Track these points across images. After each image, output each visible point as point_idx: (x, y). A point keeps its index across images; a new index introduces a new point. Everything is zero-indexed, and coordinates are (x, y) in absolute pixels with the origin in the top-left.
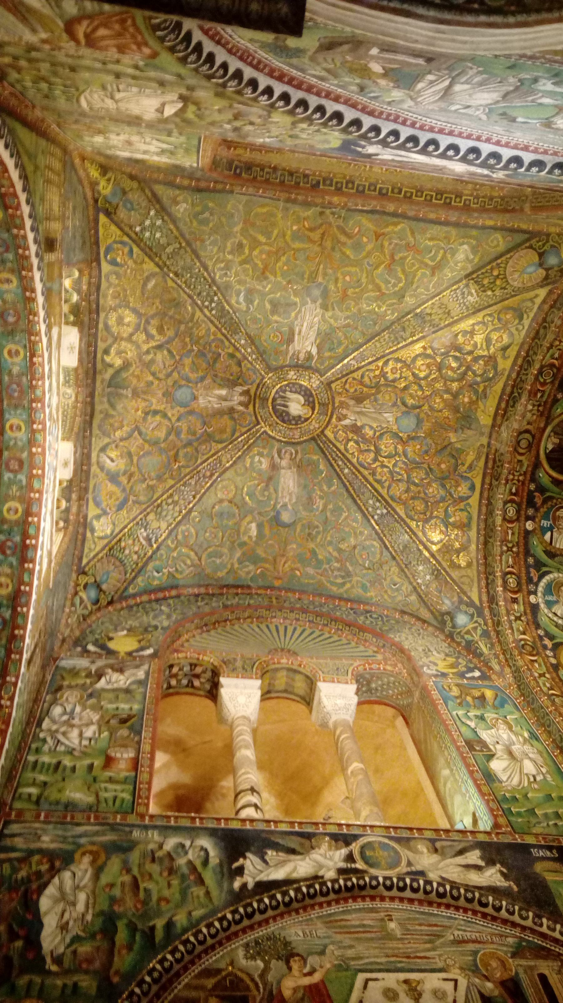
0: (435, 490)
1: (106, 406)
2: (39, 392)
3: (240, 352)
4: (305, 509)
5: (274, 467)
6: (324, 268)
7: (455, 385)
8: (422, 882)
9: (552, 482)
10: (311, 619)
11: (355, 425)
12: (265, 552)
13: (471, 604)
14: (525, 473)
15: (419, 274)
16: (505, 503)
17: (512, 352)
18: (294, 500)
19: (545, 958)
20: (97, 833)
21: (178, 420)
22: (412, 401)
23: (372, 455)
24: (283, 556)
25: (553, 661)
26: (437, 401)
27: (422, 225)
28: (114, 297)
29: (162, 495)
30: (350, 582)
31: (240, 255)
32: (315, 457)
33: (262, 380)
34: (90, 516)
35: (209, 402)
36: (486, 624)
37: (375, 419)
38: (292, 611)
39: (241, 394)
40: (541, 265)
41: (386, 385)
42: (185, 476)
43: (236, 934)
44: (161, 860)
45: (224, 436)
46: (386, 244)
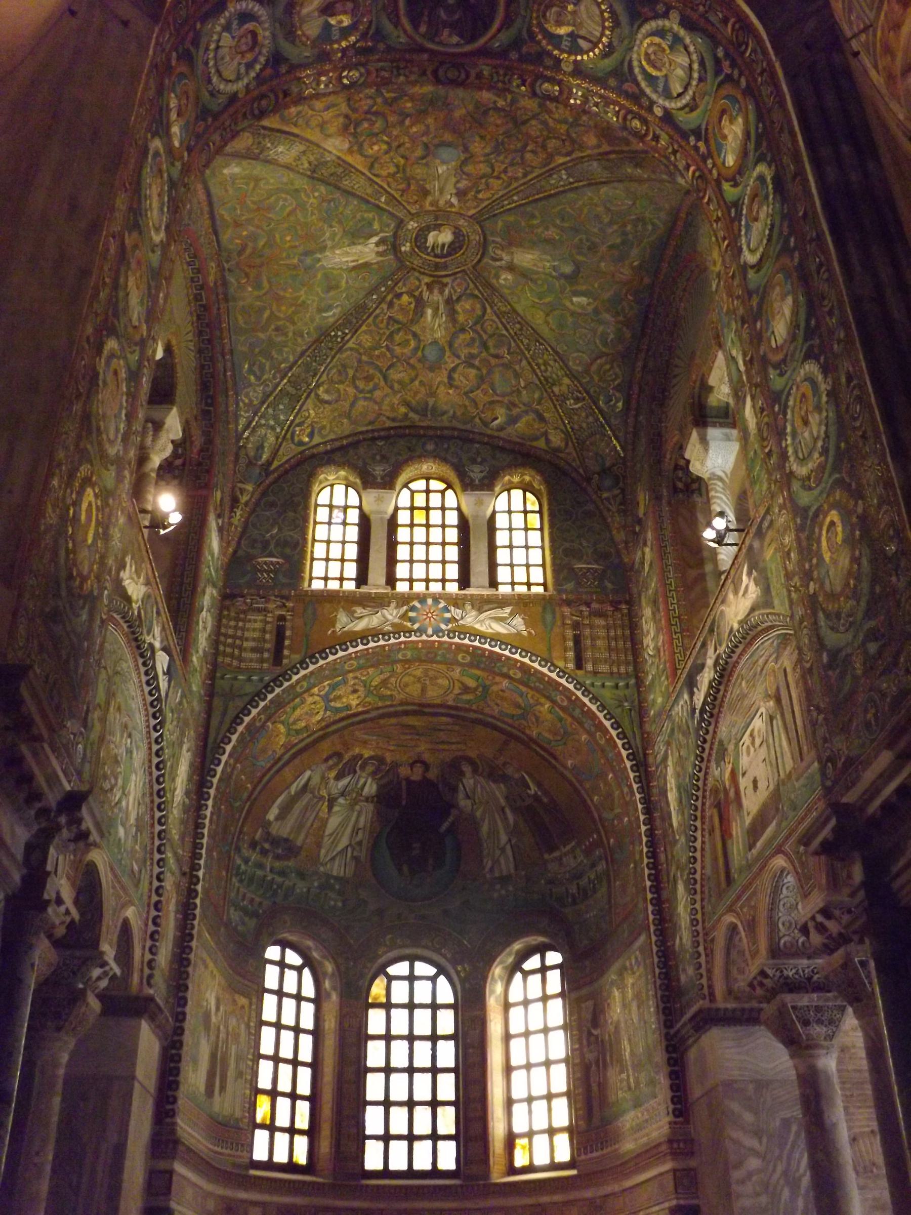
0: (534, 128)
1: (445, 417)
5: (511, 268)
14: (495, 67)
16: (534, 94)
18: (549, 258)
21: (458, 357)
23: (491, 180)
24: (613, 276)
25: (715, 172)
27: (215, 199)
28: (342, 424)
35: (439, 326)
37: (447, 180)
41: (404, 171)
43: (710, 755)
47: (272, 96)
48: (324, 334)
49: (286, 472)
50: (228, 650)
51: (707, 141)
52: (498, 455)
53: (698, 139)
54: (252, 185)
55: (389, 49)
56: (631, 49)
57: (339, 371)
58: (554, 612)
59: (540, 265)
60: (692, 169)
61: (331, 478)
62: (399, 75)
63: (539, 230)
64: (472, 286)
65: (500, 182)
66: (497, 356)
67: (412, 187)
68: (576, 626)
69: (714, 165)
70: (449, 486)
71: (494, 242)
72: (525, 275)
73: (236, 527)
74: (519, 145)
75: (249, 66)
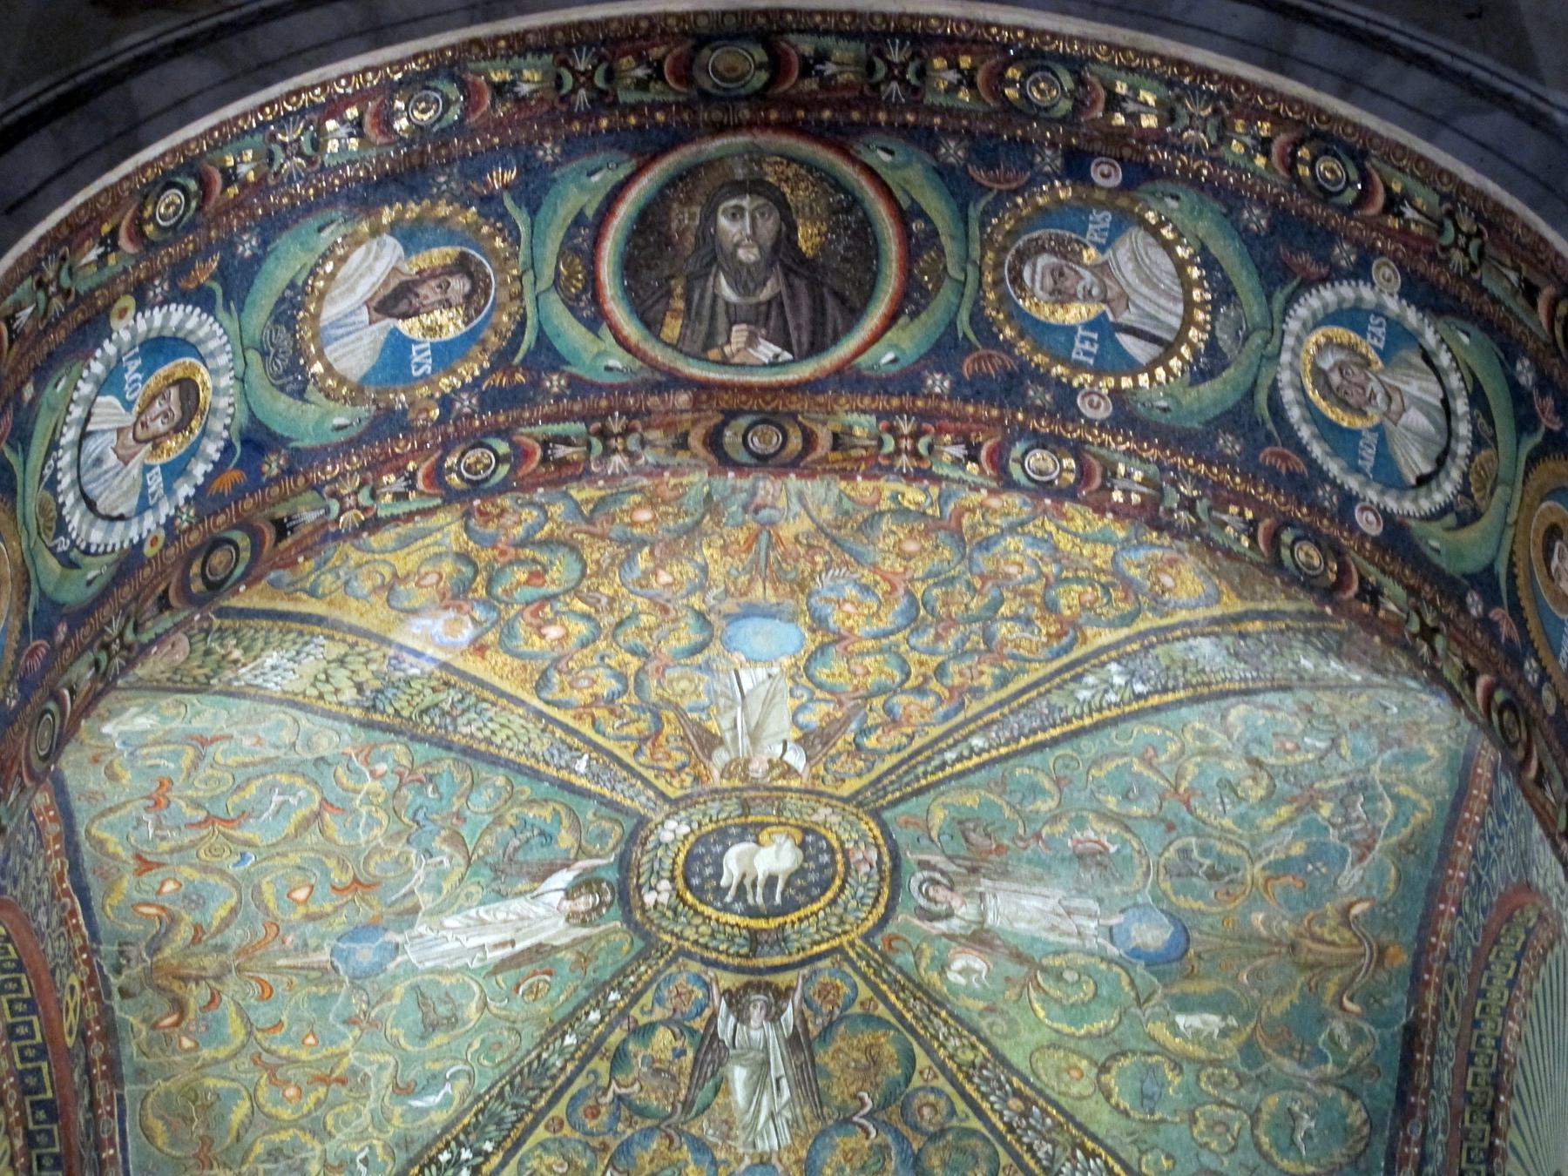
5: (980, 938)
6: (286, 954)
9: (914, 315)
11: (805, 741)
12: (1280, 991)
23: (900, 700)
24: (1293, 947)
26: (664, 578)
31: (303, 1147)
32: (939, 817)
33: (689, 955)
35: (772, 1116)
37: (768, 702)
38: (1482, 994)
39: (742, 1018)
45: (889, 1049)
46: (165, 846)
47: (242, 540)
51: (1516, 609)
53: (1491, 599)
54: (190, 753)
55: (578, 386)
60: (1483, 681)
62: (608, 452)
63: (1060, 828)
64: (865, 992)
65: (931, 700)
67: (667, 729)
69: (1544, 677)
71: (924, 865)
75: (175, 471)
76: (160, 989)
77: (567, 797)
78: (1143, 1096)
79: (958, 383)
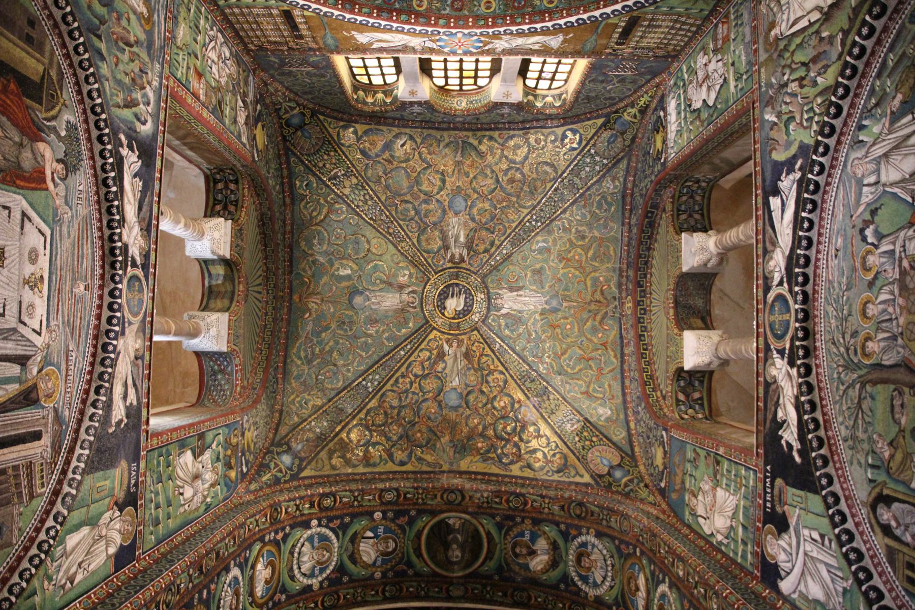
0: (395, 431)
1: (447, 141)
2: (519, 20)
3: (496, 250)
4: (366, 317)
5: (401, 287)
7: (491, 432)
8: (117, 328)
10: (268, 326)
11: (444, 355)
12: (325, 284)
13: (301, 470)
14: (424, 504)
15: (581, 382)
16: (397, 490)
17: (528, 473)
18: (373, 307)
19: (53, 448)
20: (159, 32)
21: (438, 201)
22: (472, 399)
23: (420, 373)
24: (322, 300)
25: (267, 539)
26: (475, 421)
27: (619, 376)
28: (536, 141)
29: (372, 190)
30: (302, 364)
32: (411, 325)
33: (474, 273)
34: (357, 126)
36: (285, 482)
37: (452, 371)
38: (274, 308)
39: (461, 255)
40: (612, 467)
42: (388, 211)
43: (86, 121)
44: (141, 77)
46: (600, 352)
48: (547, 226)
49: (590, 113)
50: (687, 27)
52: (398, 116)
54: (591, 389)
55: (493, 516)
56: (340, 547)
57: (536, 190)
58: (324, 43)
59: (379, 299)
61: (549, 99)
62: (487, 498)
64: (430, 260)
66: (407, 202)
68: (301, 37)
70: (441, 88)
71: (415, 307)
72: (391, 285)
73: (646, 93)
74: (402, 414)
76: (606, 299)
77: (500, 335)
78: (358, 243)
79: (408, 514)
